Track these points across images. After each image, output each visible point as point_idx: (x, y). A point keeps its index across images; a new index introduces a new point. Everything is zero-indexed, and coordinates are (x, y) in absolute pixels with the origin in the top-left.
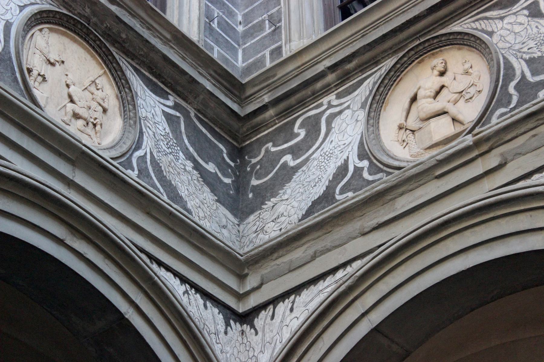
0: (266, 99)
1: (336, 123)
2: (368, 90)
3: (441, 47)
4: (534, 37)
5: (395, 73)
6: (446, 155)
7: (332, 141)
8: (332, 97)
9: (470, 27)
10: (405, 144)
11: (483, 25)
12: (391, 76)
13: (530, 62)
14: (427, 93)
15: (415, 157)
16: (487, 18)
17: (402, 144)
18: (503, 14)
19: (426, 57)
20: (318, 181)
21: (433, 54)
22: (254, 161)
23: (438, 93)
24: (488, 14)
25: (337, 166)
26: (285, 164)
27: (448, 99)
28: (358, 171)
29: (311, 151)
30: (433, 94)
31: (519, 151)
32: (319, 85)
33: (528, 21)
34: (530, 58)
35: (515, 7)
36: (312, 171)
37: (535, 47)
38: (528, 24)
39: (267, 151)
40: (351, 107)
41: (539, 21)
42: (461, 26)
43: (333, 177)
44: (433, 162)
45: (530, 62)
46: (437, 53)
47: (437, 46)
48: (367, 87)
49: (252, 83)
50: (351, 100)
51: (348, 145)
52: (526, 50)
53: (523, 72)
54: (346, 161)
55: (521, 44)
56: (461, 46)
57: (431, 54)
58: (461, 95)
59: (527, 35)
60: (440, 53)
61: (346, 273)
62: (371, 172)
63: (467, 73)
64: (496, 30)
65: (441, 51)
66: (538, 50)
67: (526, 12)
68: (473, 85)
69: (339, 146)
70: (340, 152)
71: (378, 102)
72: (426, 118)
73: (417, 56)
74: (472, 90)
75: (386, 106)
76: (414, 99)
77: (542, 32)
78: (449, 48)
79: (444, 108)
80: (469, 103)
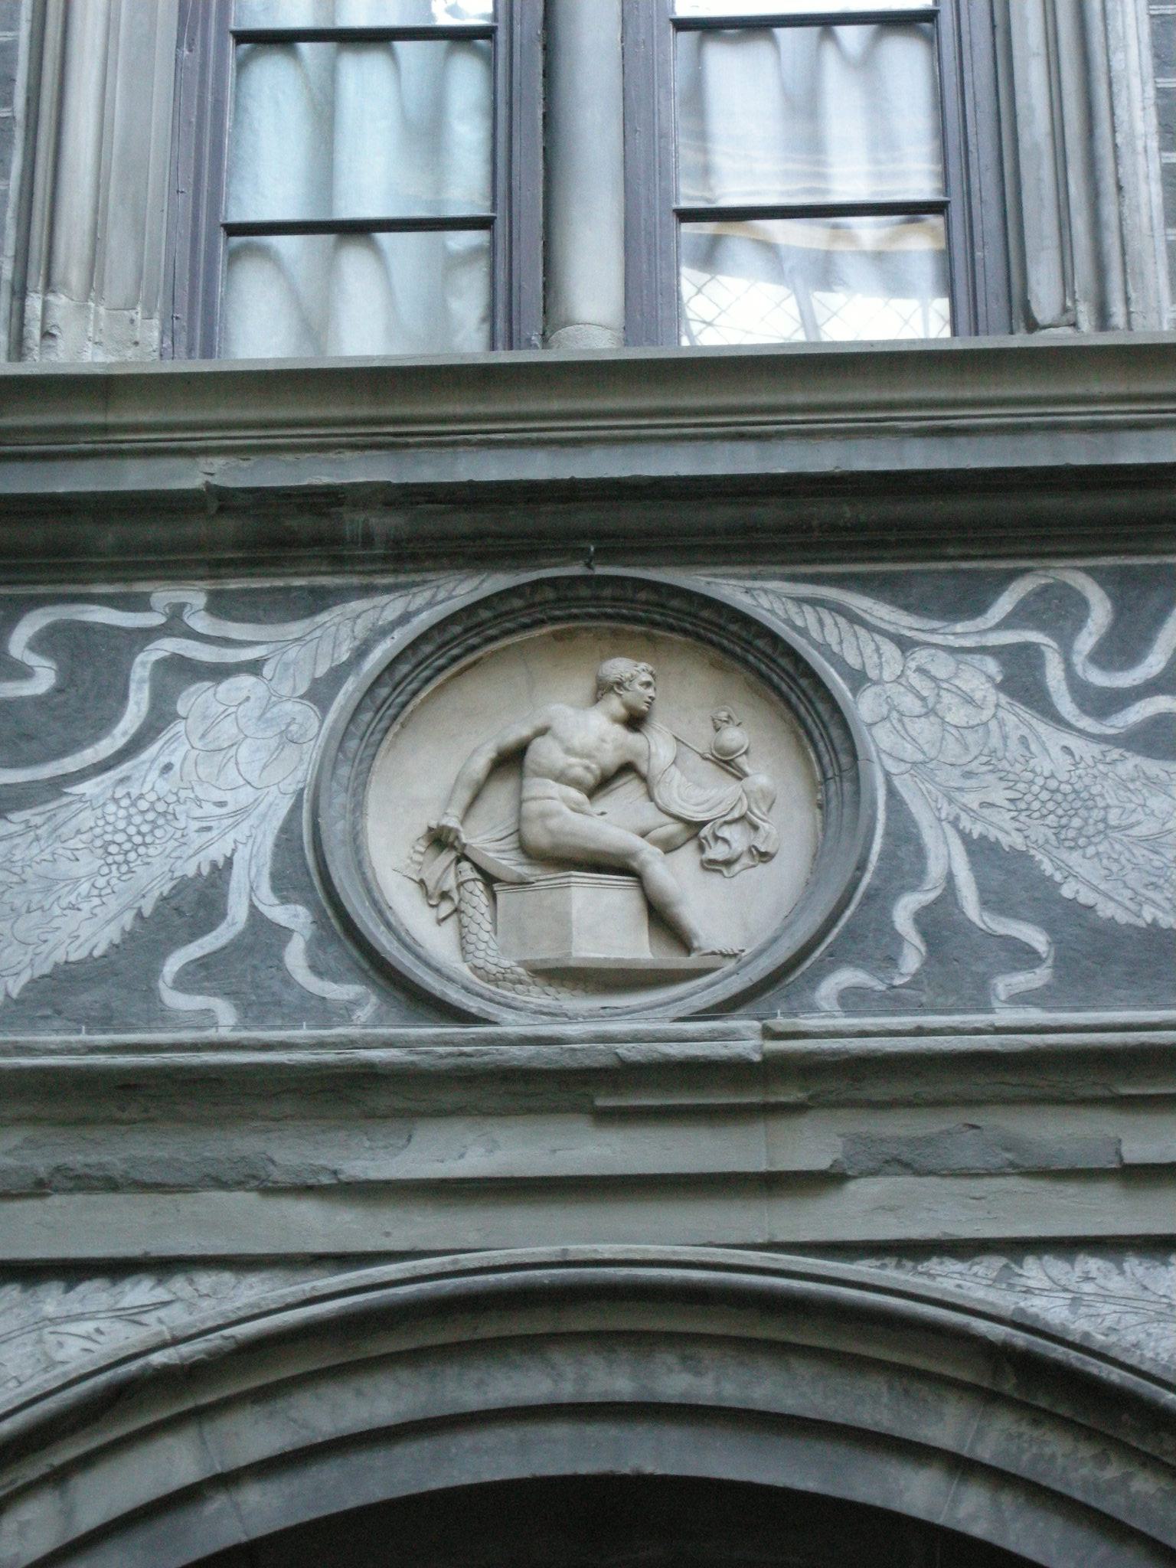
3: (655, 624)
4: (1008, 772)
6: (655, 1055)
7: (168, 768)
8: (194, 597)
10: (446, 908)
11: (832, 631)
12: (447, 636)
13: (980, 850)
14: (571, 766)
15: (489, 981)
16: (854, 619)
17: (433, 902)
18: (911, 629)
19: (586, 629)
20: (88, 896)
21: (615, 633)
25: (178, 874)
29: (70, 764)
30: (590, 779)
31: (906, 1156)
33: (997, 706)
34: (983, 838)
35: (959, 628)
36: (71, 844)
37: (1010, 810)
38: (994, 716)
40: (267, 671)
41: (1034, 722)
43: (157, 910)
45: (980, 850)
46: (632, 635)
50: (272, 647)
51: (235, 813)
52: (975, 806)
53: (950, 877)
54: (222, 871)
55: (957, 772)
57: (609, 628)
59: (986, 751)
61: (166, 1297)
64: (872, 673)
66: (1017, 825)
67: (992, 666)
68: (742, 818)
69: (199, 803)
70: (197, 825)
71: (379, 709)
74: (738, 838)
77: (1038, 770)
79: (633, 855)
80: (716, 878)
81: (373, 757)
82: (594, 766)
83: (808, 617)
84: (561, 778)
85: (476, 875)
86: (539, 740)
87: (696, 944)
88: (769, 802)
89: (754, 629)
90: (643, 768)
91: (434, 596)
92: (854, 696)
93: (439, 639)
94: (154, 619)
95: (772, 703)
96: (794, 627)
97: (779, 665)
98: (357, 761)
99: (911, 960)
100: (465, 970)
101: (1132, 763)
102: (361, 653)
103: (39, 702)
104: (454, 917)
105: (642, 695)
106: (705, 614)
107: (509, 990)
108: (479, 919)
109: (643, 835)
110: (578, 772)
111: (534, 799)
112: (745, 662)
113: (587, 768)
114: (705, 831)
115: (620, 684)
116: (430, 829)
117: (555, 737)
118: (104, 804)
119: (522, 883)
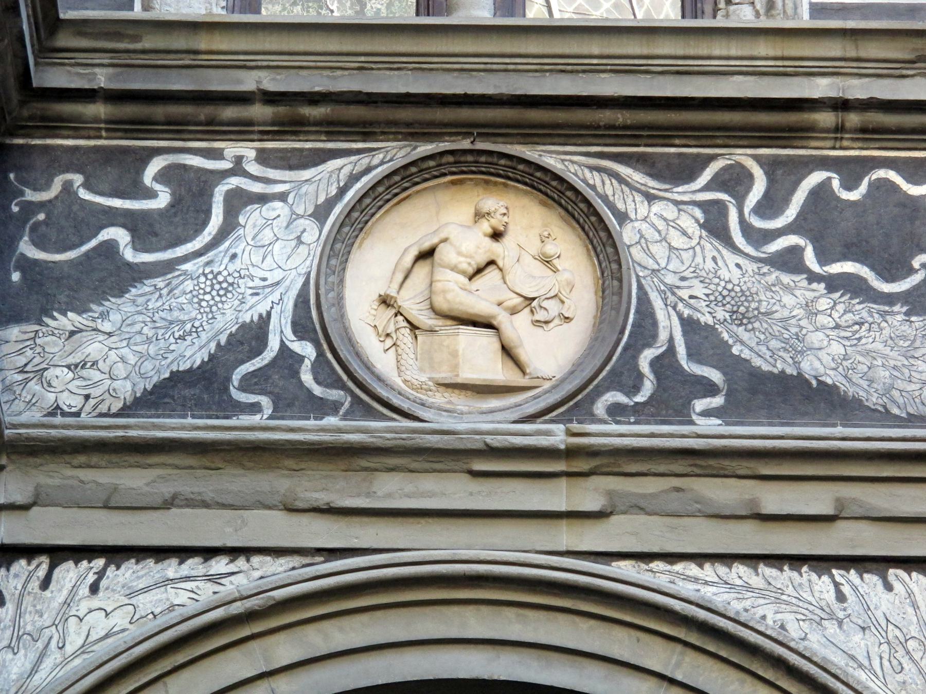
0: (102, 79)
1: (251, 217)
2: (335, 185)
3: (509, 178)
4: (706, 278)
5: (402, 179)
6: (507, 443)
7: (234, 256)
8: (247, 150)
9: (580, 173)
10: (389, 342)
11: (609, 187)
13: (689, 325)
14: (460, 262)
15: (413, 389)
16: (621, 180)
17: (382, 339)
18: (654, 188)
19: (471, 179)
20: (191, 332)
21: (487, 182)
22: (31, 196)
23: (479, 271)
24: (624, 170)
25: (240, 320)
26: (110, 248)
27: (501, 299)
28: (286, 355)
29: (180, 251)
30: (471, 271)
31: (642, 504)
32: (230, 112)
33: (701, 237)
34: (690, 317)
35: (680, 189)
36: (180, 300)
37: (705, 301)
38: (699, 243)
39: (67, 187)
40: (290, 199)
41: (720, 248)
42: (563, 161)
43: (229, 341)
44: (476, 443)
45: (689, 325)
46: (496, 184)
47: (501, 172)
48: (335, 176)
49: (81, 27)
50: (293, 184)
51: (272, 285)
52: (686, 297)
53: (671, 340)
54: (265, 320)
55: (678, 276)
56: (550, 202)
57: (483, 179)
58: (527, 302)
59: (693, 265)
60: (501, 186)
61: (236, 570)
62: (321, 378)
63: (547, 262)
64: (632, 216)
65: (505, 185)
66: (709, 310)
67: (698, 213)
68: (556, 296)
69: (252, 277)
70: (251, 291)
71: (353, 225)
72: (448, 313)
73: (454, 169)
74: (553, 307)
75: (364, 239)
76: (427, 255)
77: (722, 277)
78: (523, 190)
79: (494, 317)
80: (540, 330)
81: (349, 252)
82: (473, 263)
83: (595, 178)
84: (454, 269)
85: (405, 324)
86: (442, 245)
87: (528, 371)
88: (571, 287)
89: (565, 185)
90: (500, 263)
91: (384, 158)
92: (621, 227)
93: (387, 183)
94: (225, 165)
95: (574, 228)
96: (588, 185)
97: (578, 207)
98: (340, 255)
99: (648, 388)
100: (398, 382)
101: (774, 275)
102: (342, 191)
103: (161, 212)
104: (393, 348)
105: (501, 221)
106: (538, 174)
107: (424, 395)
108: (408, 351)
109: (499, 304)
110: (464, 266)
111: (439, 281)
112: (560, 205)
113: (469, 264)
114: (535, 303)
115: (488, 214)
116: (380, 296)
117: (451, 244)
118: (199, 277)
119: (432, 331)
